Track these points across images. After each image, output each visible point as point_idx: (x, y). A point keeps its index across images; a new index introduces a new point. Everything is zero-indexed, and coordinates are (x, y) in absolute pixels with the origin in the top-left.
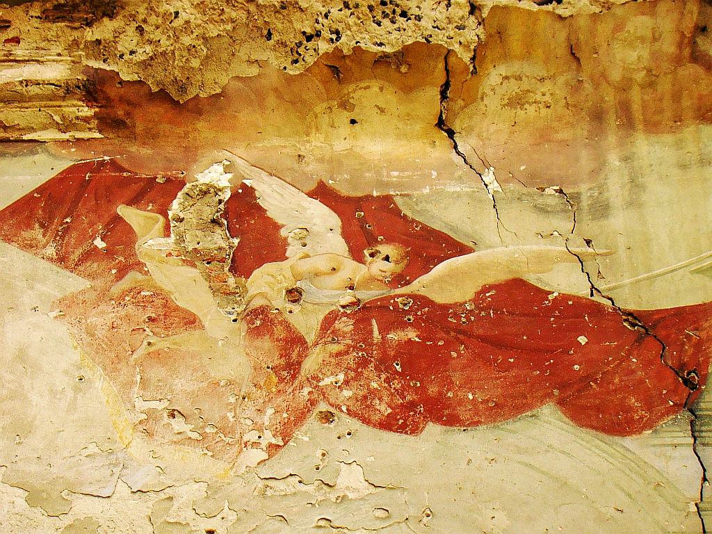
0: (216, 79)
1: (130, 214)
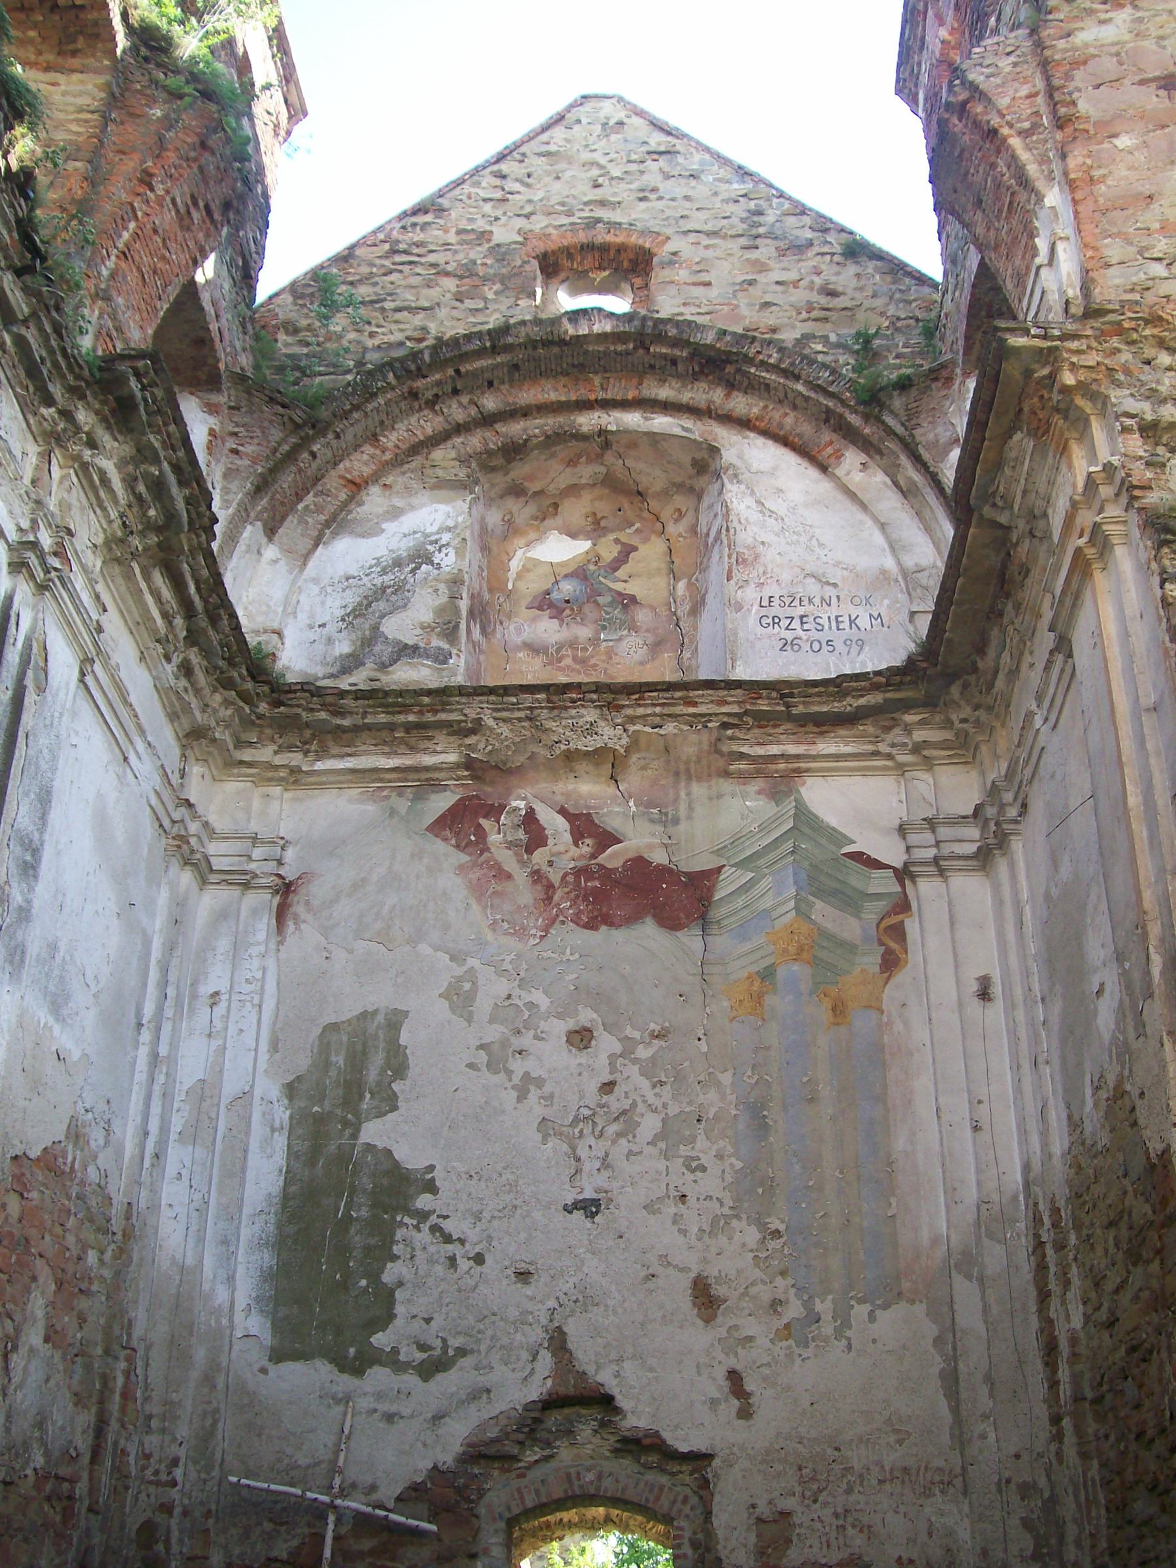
1: (484, 822)
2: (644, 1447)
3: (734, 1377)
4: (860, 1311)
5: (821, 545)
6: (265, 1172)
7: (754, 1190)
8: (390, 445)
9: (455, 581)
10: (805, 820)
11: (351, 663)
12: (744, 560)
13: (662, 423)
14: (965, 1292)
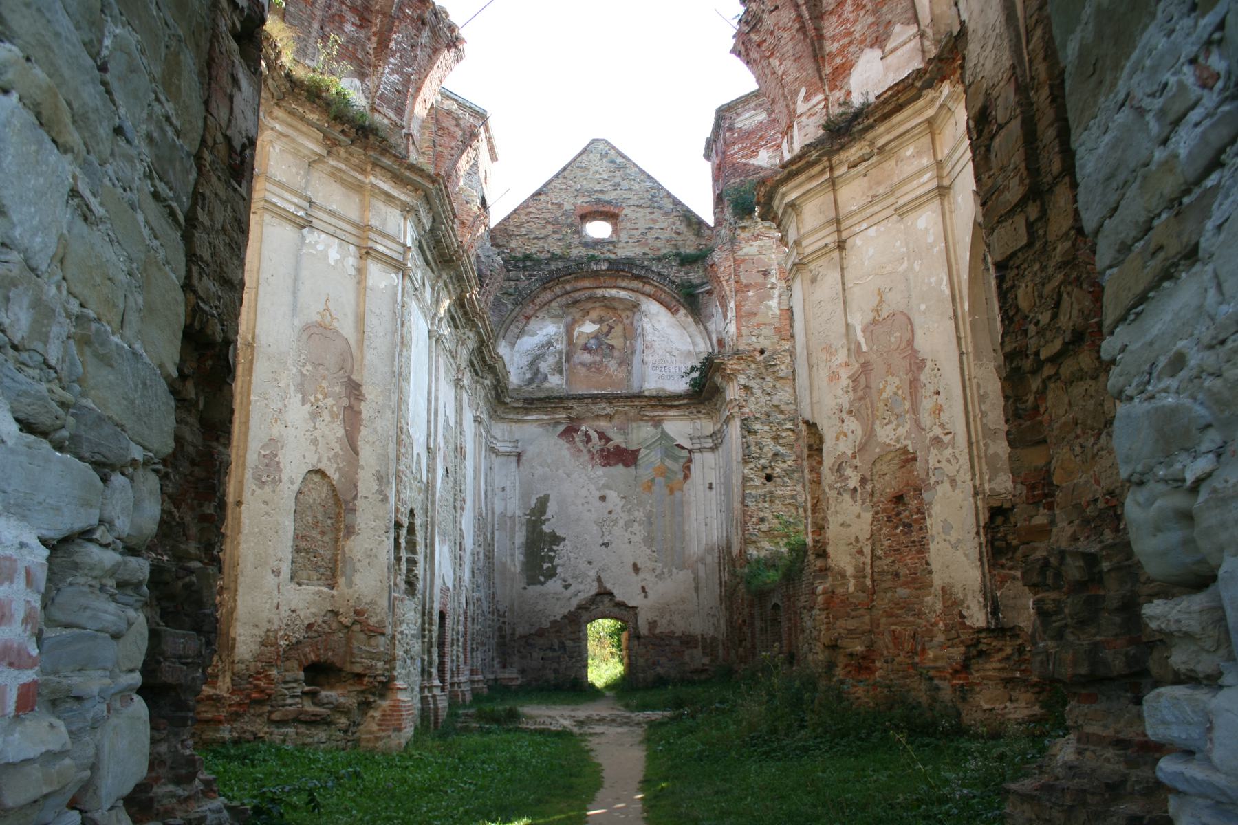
2: (621, 605)
3: (643, 589)
4: (674, 571)
6: (520, 537)
7: (649, 541)
9: (561, 353)
11: (531, 381)
13: (623, 294)
14: (701, 568)
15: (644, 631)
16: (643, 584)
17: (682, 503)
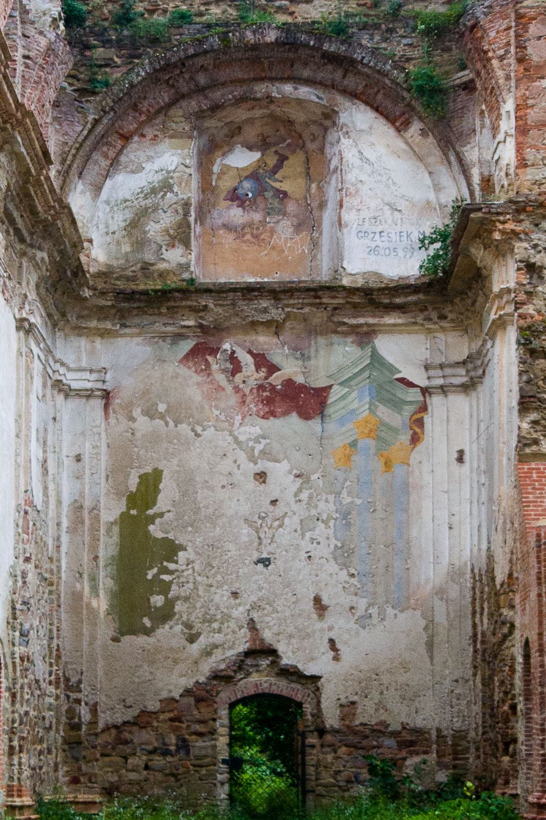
0: (227, 324)
1: (210, 359)
2: (291, 674)
3: (332, 642)
4: (390, 611)
5: (394, 184)
6: (108, 547)
7: (343, 555)
8: (144, 109)
9: (187, 205)
10: (376, 358)
12: (350, 193)
13: (304, 92)
15: (332, 719)
16: (332, 635)
17: (406, 488)
